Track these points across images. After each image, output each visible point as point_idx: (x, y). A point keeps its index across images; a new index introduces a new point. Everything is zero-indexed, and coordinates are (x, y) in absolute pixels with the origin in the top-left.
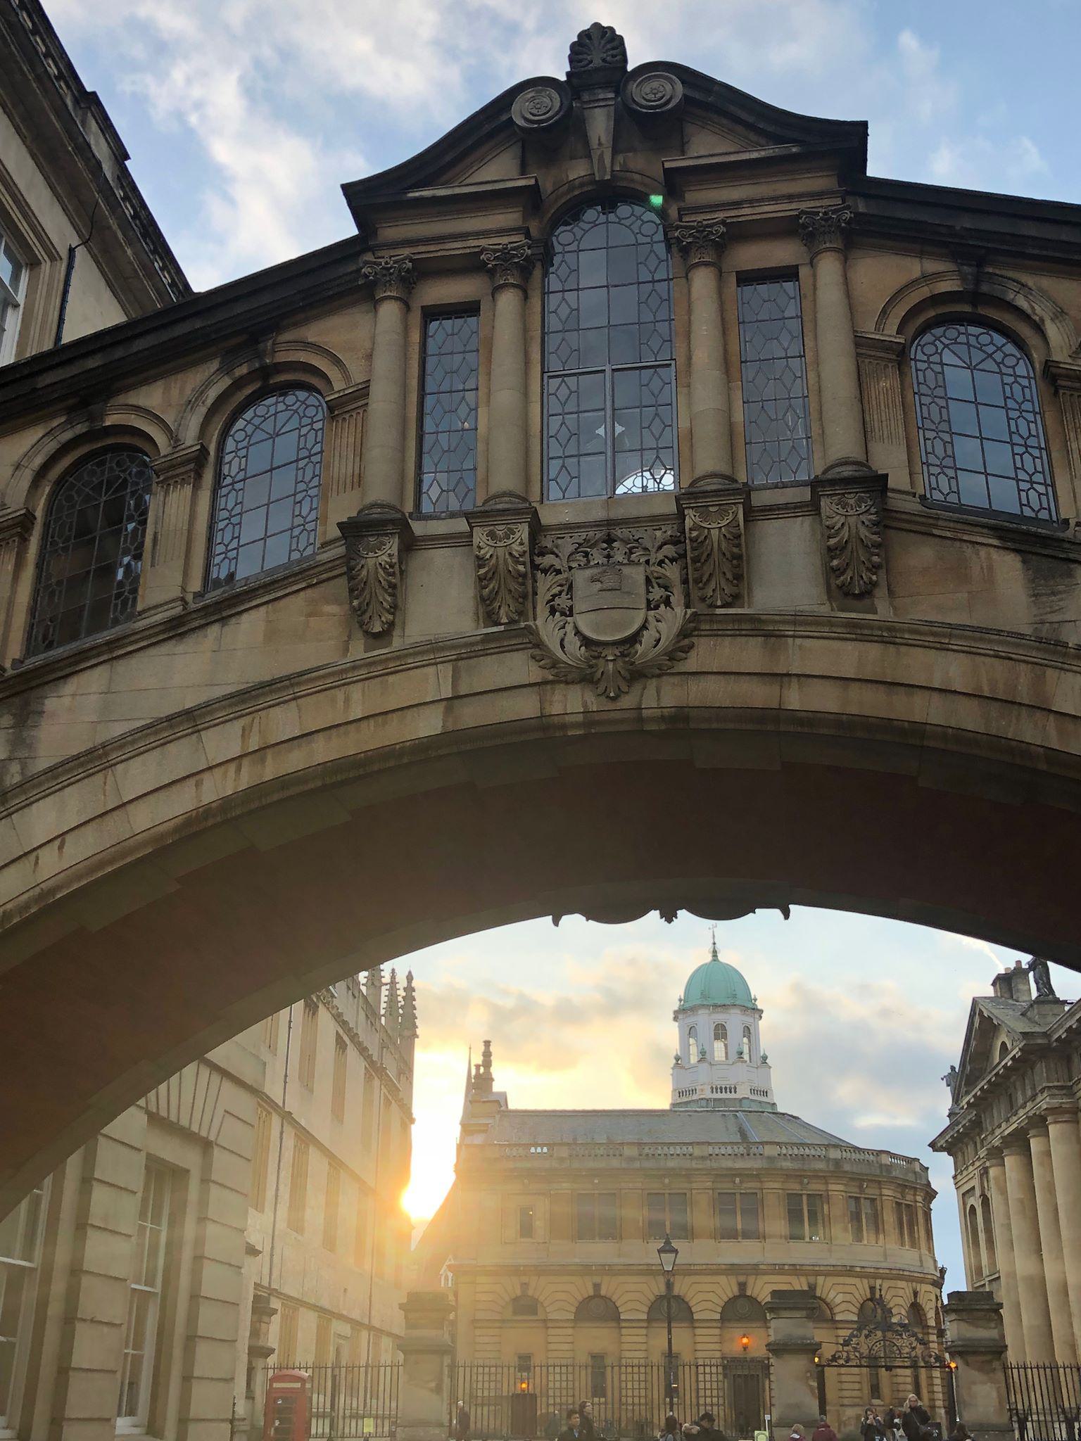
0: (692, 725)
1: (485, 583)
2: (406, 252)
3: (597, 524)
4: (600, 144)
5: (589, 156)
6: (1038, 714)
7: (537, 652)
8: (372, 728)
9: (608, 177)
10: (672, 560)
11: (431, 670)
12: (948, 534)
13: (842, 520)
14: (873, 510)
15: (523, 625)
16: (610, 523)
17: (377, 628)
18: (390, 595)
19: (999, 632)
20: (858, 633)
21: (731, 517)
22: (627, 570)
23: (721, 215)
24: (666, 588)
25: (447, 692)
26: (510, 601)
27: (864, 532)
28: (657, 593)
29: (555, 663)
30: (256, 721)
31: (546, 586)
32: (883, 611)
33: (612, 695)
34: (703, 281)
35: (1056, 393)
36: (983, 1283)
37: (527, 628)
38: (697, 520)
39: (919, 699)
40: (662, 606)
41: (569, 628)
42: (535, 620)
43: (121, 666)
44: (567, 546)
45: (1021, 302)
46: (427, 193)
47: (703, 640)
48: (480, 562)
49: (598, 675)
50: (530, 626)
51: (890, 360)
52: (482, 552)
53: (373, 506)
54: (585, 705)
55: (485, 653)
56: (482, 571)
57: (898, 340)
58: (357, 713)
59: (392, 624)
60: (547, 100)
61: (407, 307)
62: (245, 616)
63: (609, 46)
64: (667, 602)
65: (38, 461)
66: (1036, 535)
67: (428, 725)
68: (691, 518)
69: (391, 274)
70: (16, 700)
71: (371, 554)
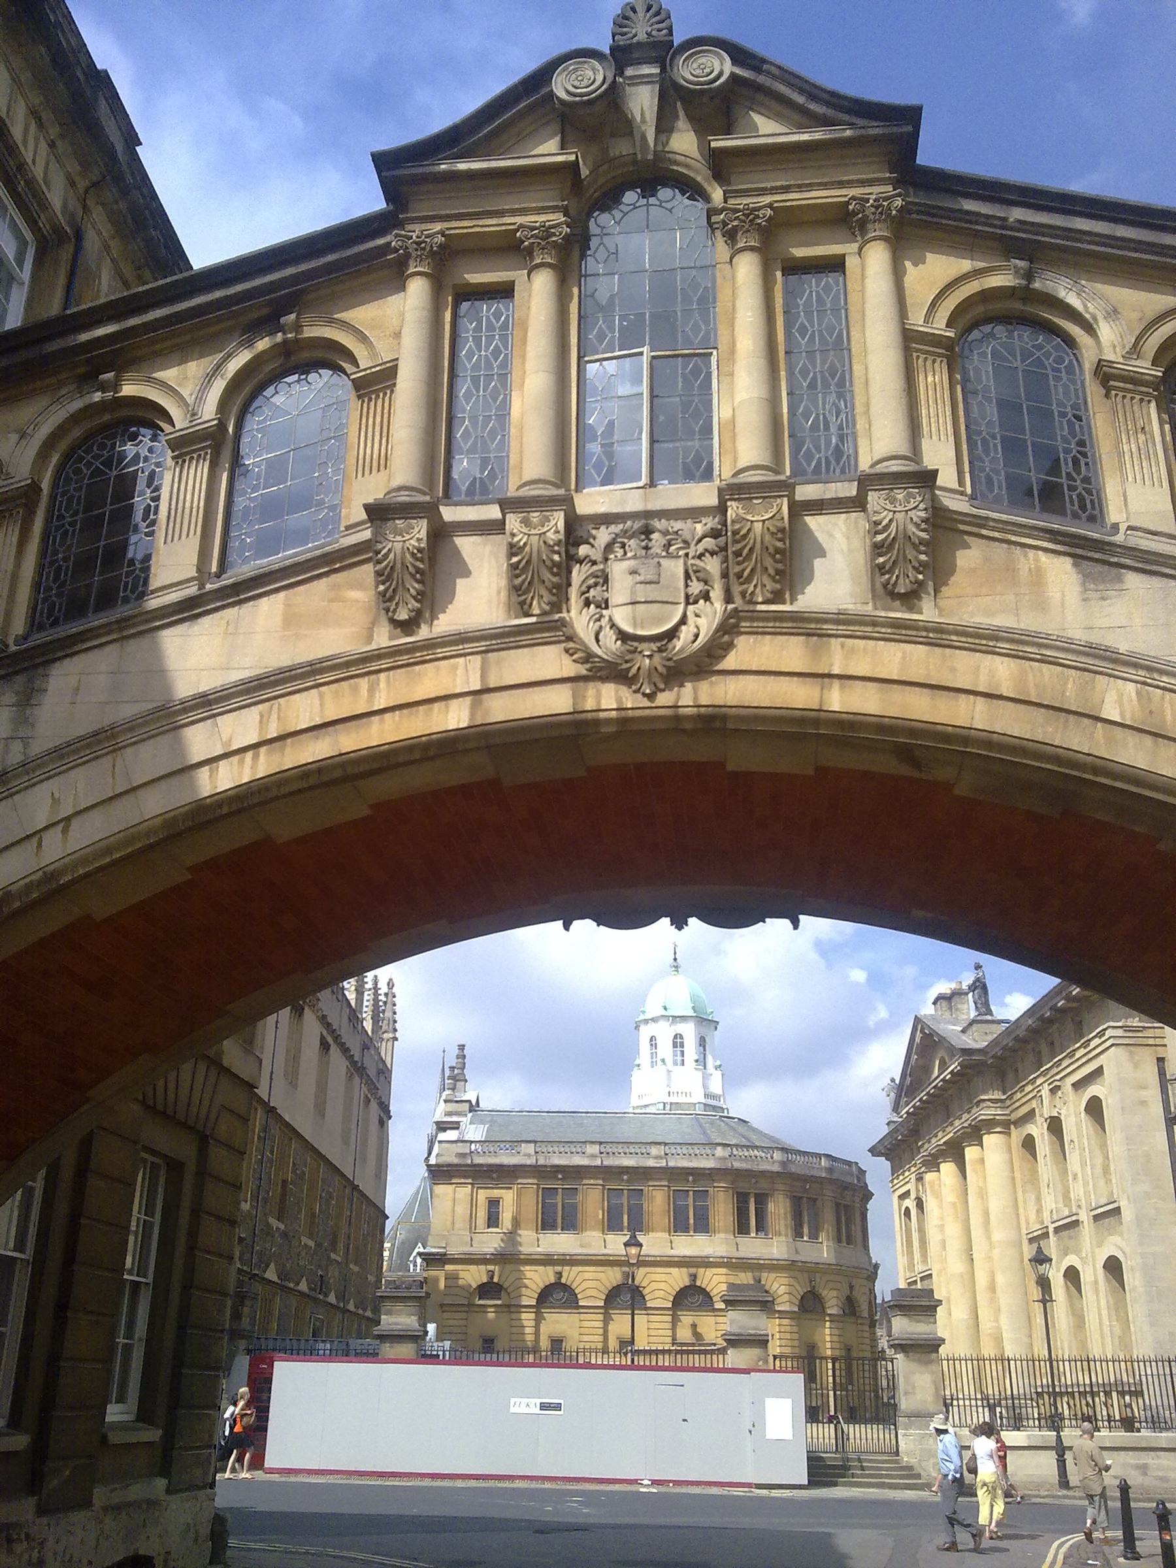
0: (730, 726)
1: (518, 572)
2: (438, 227)
3: (634, 516)
7: (571, 645)
8: (397, 718)
10: (712, 554)
11: (461, 660)
12: (996, 535)
13: (891, 515)
14: (922, 506)
15: (557, 616)
16: (648, 514)
17: (403, 615)
18: (418, 581)
20: (903, 632)
21: (775, 510)
22: (664, 562)
23: (767, 199)
24: (706, 583)
26: (544, 592)
27: (912, 529)
28: (696, 587)
29: (589, 657)
30: (276, 707)
31: (578, 574)
32: (928, 612)
33: (648, 691)
34: (747, 268)
35: (1107, 396)
37: (562, 620)
38: (741, 511)
40: (702, 602)
41: (605, 621)
42: (568, 611)
44: (603, 536)
47: (742, 638)
48: (513, 550)
49: (634, 671)
50: (564, 618)
51: (939, 355)
52: (516, 539)
53: (400, 489)
54: (619, 700)
56: (515, 559)
57: (948, 334)
58: (380, 703)
60: (590, 73)
63: (654, 20)
64: (706, 597)
66: (1086, 538)
67: (456, 717)
68: (734, 509)
69: (424, 249)
70: (20, 679)
71: (399, 538)
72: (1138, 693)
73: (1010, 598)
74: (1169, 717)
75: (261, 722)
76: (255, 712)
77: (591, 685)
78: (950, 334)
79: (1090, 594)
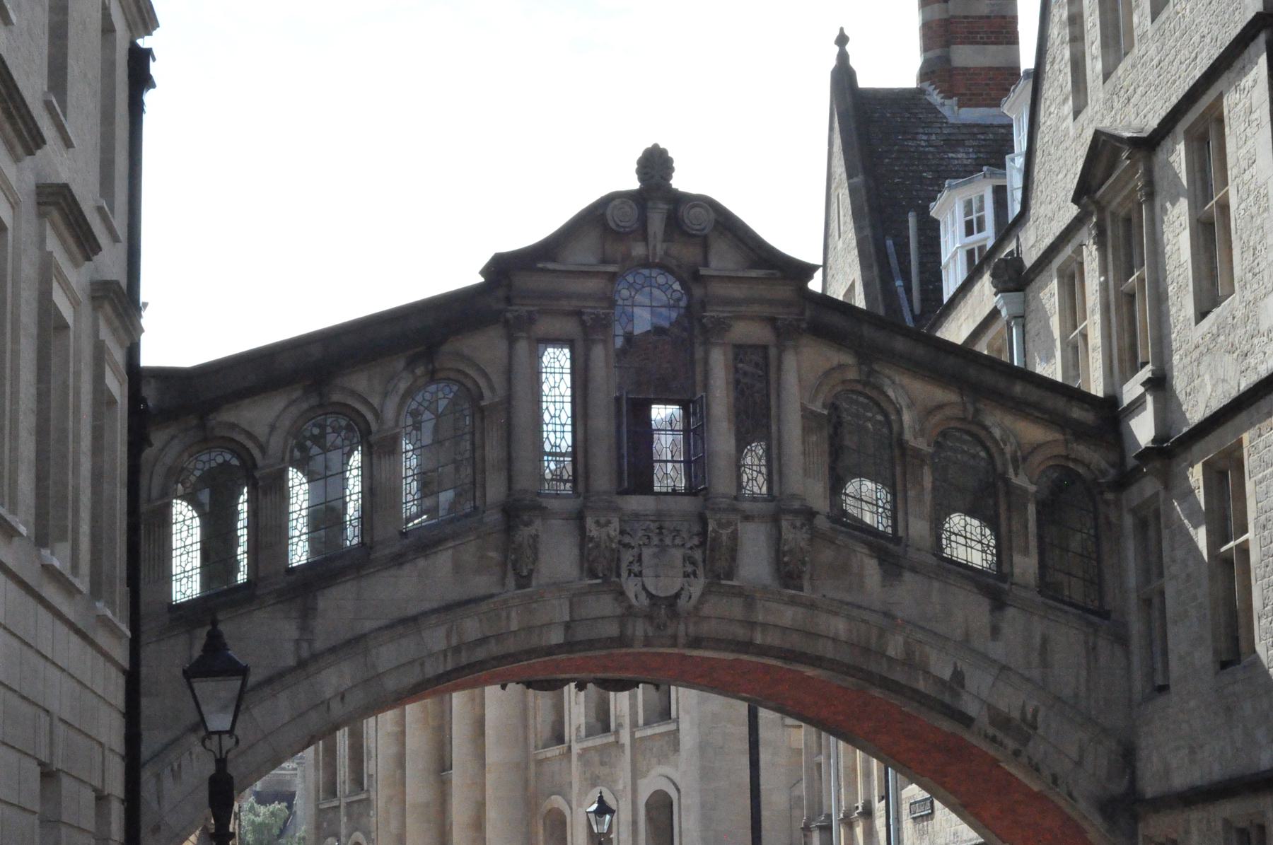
5: (645, 238)
9: (657, 260)
10: (697, 546)
17: (525, 573)
20: (793, 602)
25: (567, 618)
28: (690, 569)
29: (631, 607)
32: (807, 593)
36: (335, 803)
42: (619, 576)
45: (891, 393)
46: (550, 266)
54: (645, 631)
58: (514, 626)
61: (529, 338)
65: (286, 422)
67: (556, 637)
78: (826, 412)
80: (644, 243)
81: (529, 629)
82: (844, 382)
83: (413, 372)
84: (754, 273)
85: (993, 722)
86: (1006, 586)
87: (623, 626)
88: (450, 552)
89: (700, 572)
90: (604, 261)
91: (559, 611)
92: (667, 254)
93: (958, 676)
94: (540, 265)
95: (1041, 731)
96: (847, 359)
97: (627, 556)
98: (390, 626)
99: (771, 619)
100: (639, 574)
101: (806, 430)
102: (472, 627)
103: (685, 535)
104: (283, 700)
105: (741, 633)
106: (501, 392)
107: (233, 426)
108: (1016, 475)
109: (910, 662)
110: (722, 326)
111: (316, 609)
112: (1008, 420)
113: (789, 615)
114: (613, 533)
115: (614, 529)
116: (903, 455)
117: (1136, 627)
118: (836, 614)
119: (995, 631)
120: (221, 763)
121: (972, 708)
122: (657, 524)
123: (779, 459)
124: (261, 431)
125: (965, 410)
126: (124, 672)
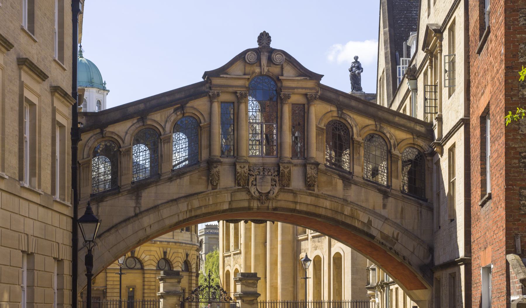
4: (264, 65)
5: (260, 66)
6: (342, 214)
9: (265, 74)
10: (277, 175)
17: (215, 184)
19: (337, 198)
20: (311, 195)
27: (314, 175)
29: (252, 196)
36: (229, 254)
37: (246, 188)
38: (283, 168)
39: (321, 209)
42: (248, 185)
43: (158, 187)
45: (349, 121)
47: (282, 193)
54: (257, 205)
55: (238, 191)
56: (238, 175)
58: (211, 202)
59: (218, 183)
60: (253, 55)
61: (218, 102)
62: (185, 178)
65: (130, 132)
67: (226, 206)
70: (136, 193)
72: (351, 209)
73: (331, 188)
74: (355, 214)
75: (187, 206)
76: (186, 204)
77: (252, 200)
78: (325, 128)
79: (345, 189)
80: (259, 67)
81: (216, 204)
82: (332, 117)
83: (176, 114)
84: (299, 78)
85: (382, 238)
86: (389, 190)
87: (249, 203)
88: (189, 176)
89: (277, 185)
90: (245, 74)
91: (227, 197)
92: (268, 71)
93: (370, 222)
94: (222, 76)
95: (399, 241)
96: (334, 109)
97: (252, 179)
98: (168, 202)
99: (303, 201)
100: (256, 185)
101: (318, 135)
102: (196, 203)
103: (272, 171)
104: (130, 227)
105: (292, 206)
106: (207, 119)
107: (112, 133)
108: (394, 150)
109: (352, 217)
110: (289, 97)
111: (142, 196)
112: (392, 131)
113: (309, 199)
114: (246, 171)
115: (246, 169)
116: (353, 143)
117: (435, 206)
118: (326, 199)
119: (384, 206)
120: (90, 251)
121: (374, 233)
122: (262, 168)
123: (307, 144)
124: (122, 134)
125: (376, 127)
126: (72, 218)
